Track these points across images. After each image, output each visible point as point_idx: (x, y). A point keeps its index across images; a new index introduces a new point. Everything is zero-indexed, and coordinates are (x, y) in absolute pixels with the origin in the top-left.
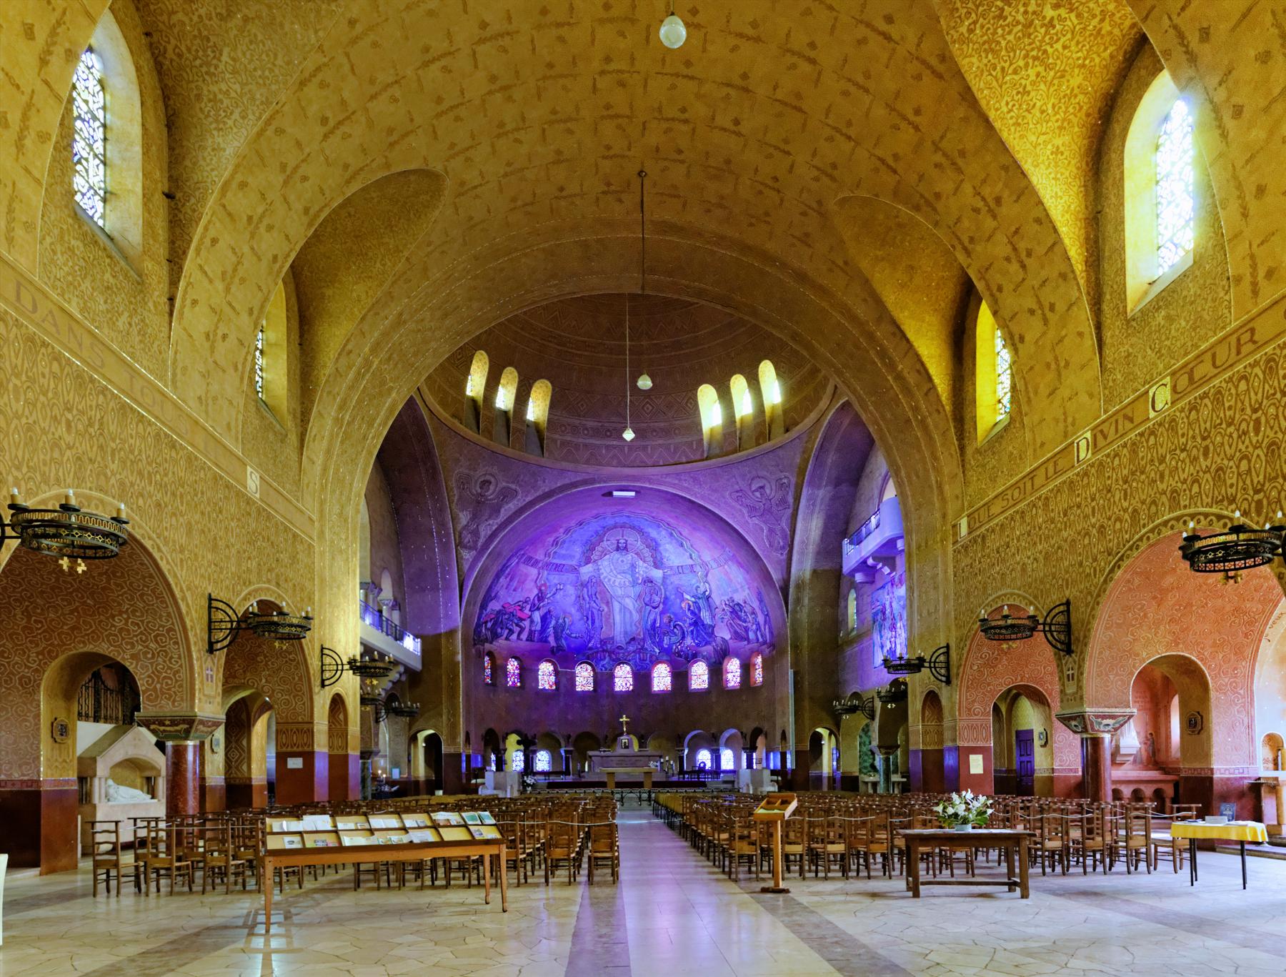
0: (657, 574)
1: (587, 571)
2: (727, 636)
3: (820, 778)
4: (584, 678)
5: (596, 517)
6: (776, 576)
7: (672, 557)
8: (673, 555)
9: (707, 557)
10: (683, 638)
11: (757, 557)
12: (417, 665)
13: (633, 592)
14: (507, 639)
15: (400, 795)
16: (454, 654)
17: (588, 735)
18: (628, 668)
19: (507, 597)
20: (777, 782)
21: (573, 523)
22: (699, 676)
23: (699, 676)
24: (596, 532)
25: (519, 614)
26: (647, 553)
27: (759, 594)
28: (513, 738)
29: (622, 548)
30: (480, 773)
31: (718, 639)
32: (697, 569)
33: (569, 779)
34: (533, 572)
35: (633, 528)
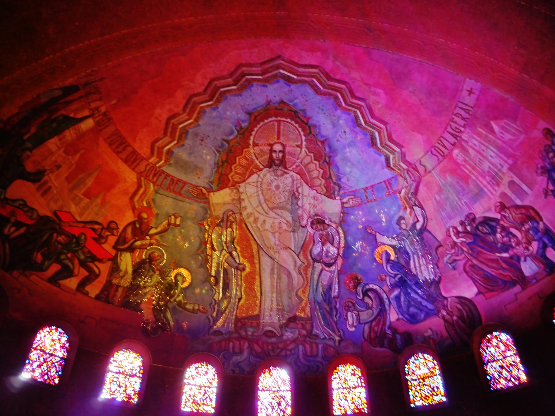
0: (332, 207)
1: (221, 198)
8: (359, 167)
13: (295, 240)
24: (238, 124)
26: (316, 171)
29: (278, 163)
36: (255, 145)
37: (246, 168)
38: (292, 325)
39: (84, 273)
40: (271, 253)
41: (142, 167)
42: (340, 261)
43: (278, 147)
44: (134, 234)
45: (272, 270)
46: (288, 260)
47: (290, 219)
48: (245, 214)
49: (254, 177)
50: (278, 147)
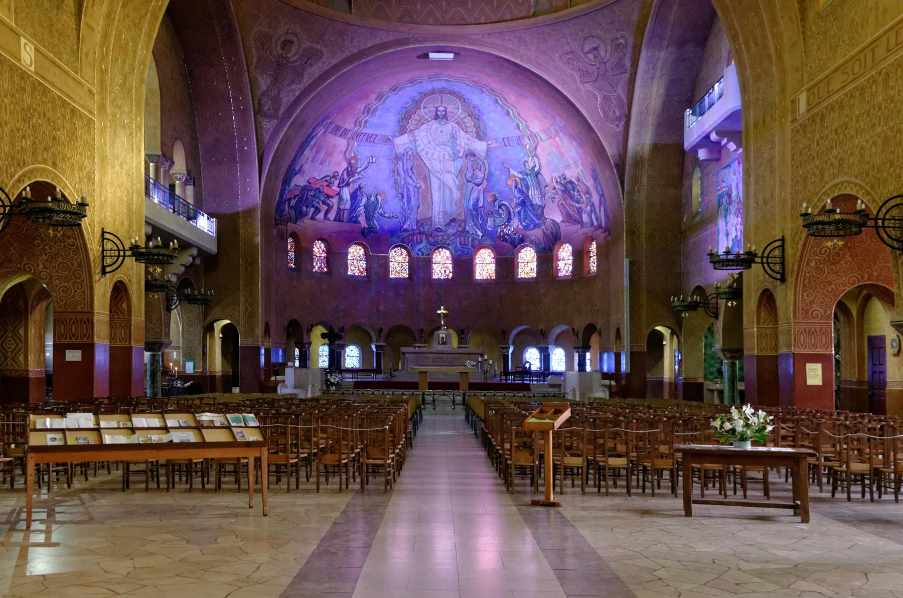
0: (480, 147)
1: (402, 141)
2: (559, 219)
3: (661, 383)
4: (398, 263)
5: (412, 81)
6: (611, 150)
9: (536, 127)
10: (509, 220)
11: (590, 129)
12: (212, 248)
13: (454, 166)
14: (313, 218)
15: (194, 392)
16: (254, 235)
17: (406, 330)
18: (448, 253)
19: (314, 170)
20: (610, 387)
21: (386, 88)
22: (527, 263)
23: (527, 263)
25: (326, 190)
27: (594, 170)
28: (319, 330)
30: (279, 369)
31: (548, 222)
32: (526, 141)
33: (380, 378)
34: (342, 143)
36: (424, 108)
37: (419, 121)
38: (452, 224)
40: (438, 175)
41: (350, 135)
42: (485, 182)
43: (441, 109)
44: (348, 175)
45: (440, 187)
46: (451, 180)
47: (451, 152)
48: (419, 149)
49: (425, 126)
50: (441, 109)
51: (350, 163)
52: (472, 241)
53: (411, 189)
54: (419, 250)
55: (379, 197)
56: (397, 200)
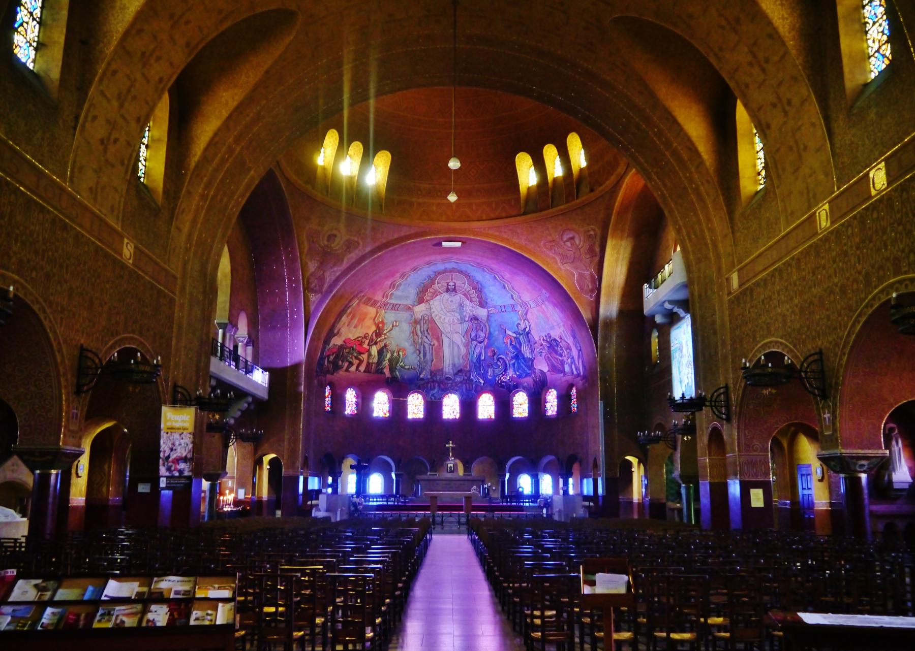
0: (482, 313)
1: (420, 310)
7: (496, 298)
26: (474, 294)
35: (461, 272)
39: (357, 362)
42: (486, 341)
44: (376, 336)
46: (459, 339)
48: (433, 315)
49: (438, 297)
50: (451, 284)
51: (378, 327)
52: (477, 386)
53: (427, 346)
54: (433, 395)
55: (401, 353)
56: (415, 355)
